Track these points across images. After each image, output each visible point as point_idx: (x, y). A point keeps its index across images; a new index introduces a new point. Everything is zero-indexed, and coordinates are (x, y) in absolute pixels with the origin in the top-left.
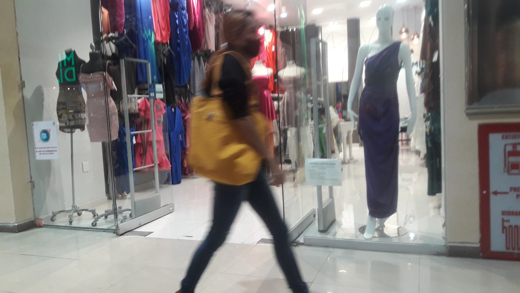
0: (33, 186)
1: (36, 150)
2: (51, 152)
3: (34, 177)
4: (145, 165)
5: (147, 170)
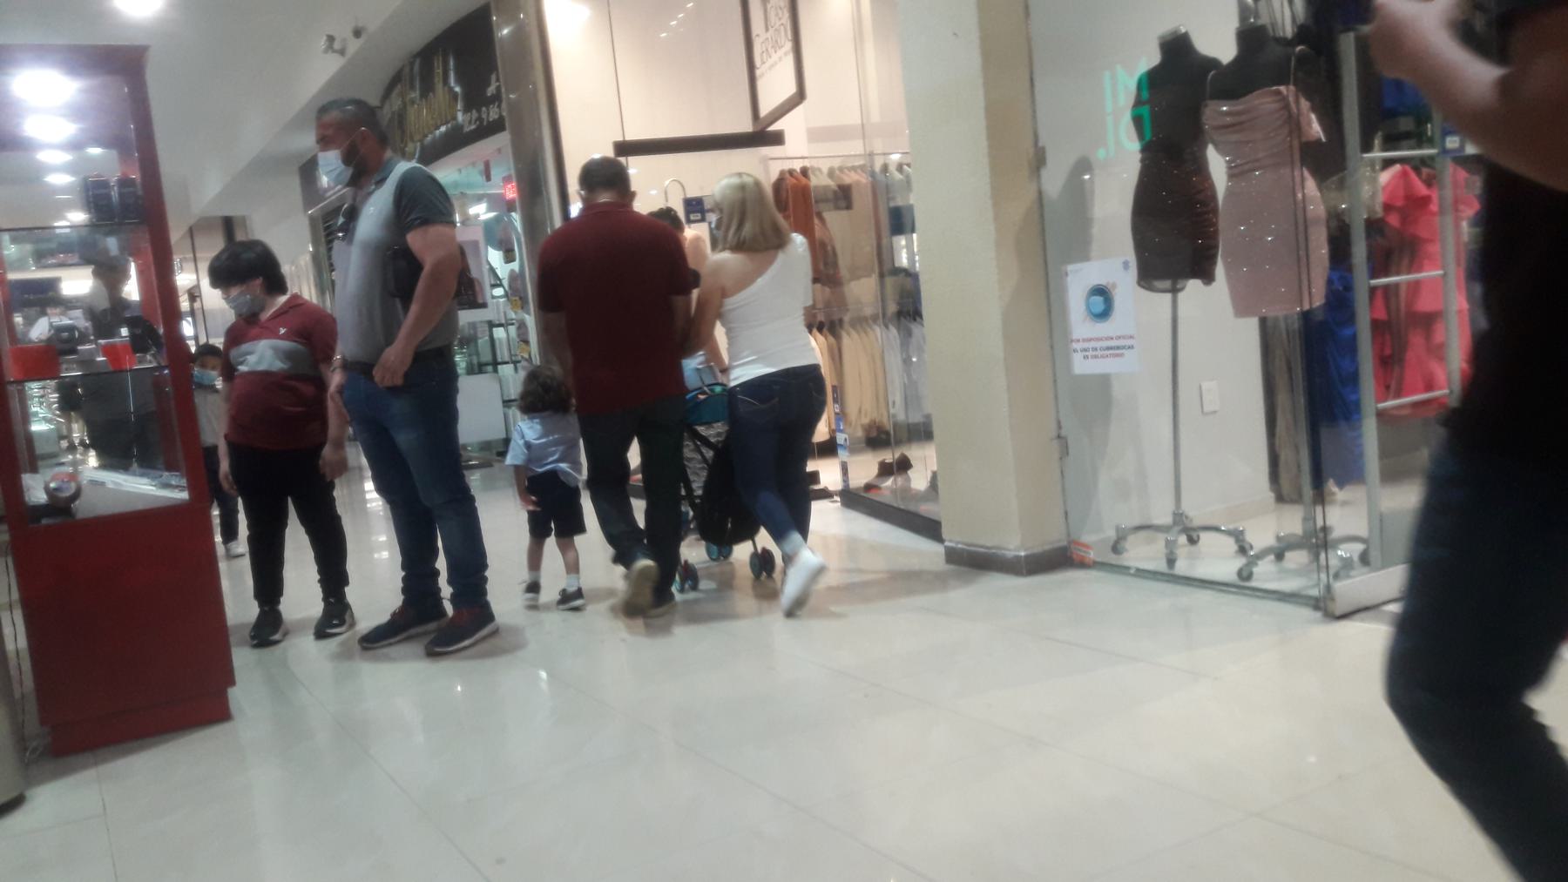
0: (1065, 451)
1: (1075, 345)
2: (1116, 351)
3: (1072, 421)
4: (1398, 395)
5: (1405, 412)
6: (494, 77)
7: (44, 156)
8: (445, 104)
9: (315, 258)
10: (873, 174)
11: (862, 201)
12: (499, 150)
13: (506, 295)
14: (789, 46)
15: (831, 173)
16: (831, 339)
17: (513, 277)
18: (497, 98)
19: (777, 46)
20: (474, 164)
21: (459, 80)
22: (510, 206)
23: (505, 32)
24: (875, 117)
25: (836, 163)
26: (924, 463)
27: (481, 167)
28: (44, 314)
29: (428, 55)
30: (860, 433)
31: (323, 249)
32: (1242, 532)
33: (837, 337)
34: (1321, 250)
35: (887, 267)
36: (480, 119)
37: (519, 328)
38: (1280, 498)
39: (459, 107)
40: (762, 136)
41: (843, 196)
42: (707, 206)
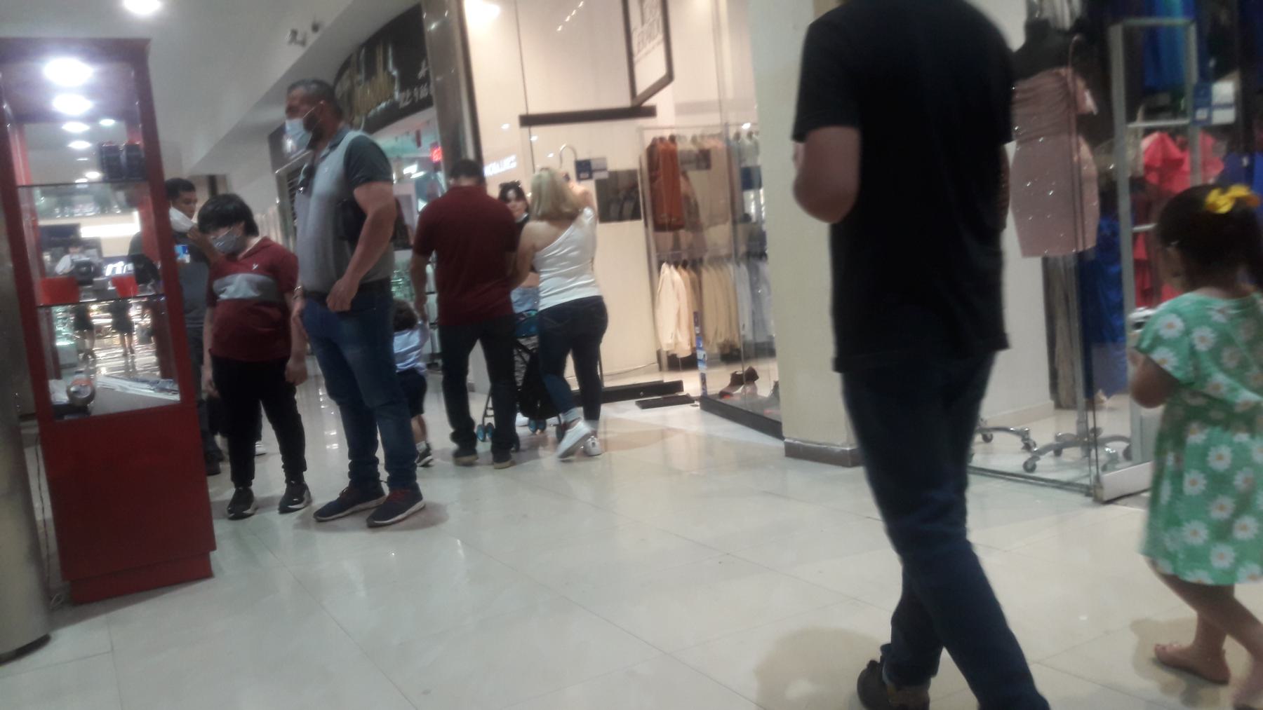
6: (424, 64)
7: (69, 127)
8: (385, 84)
9: (281, 208)
10: (727, 140)
11: (719, 163)
12: (428, 122)
14: (660, 37)
15: (694, 140)
16: (693, 274)
18: (426, 80)
19: (651, 37)
20: (408, 133)
21: (396, 65)
22: (436, 167)
23: (433, 26)
24: (730, 94)
25: (698, 132)
26: (768, 374)
27: (413, 135)
28: (67, 252)
29: (372, 45)
30: (716, 351)
31: (287, 200)
32: (1027, 432)
33: (699, 273)
34: (1093, 203)
35: (738, 216)
36: (412, 96)
38: (1059, 405)
39: (396, 87)
40: (639, 110)
41: (704, 158)
42: (594, 166)
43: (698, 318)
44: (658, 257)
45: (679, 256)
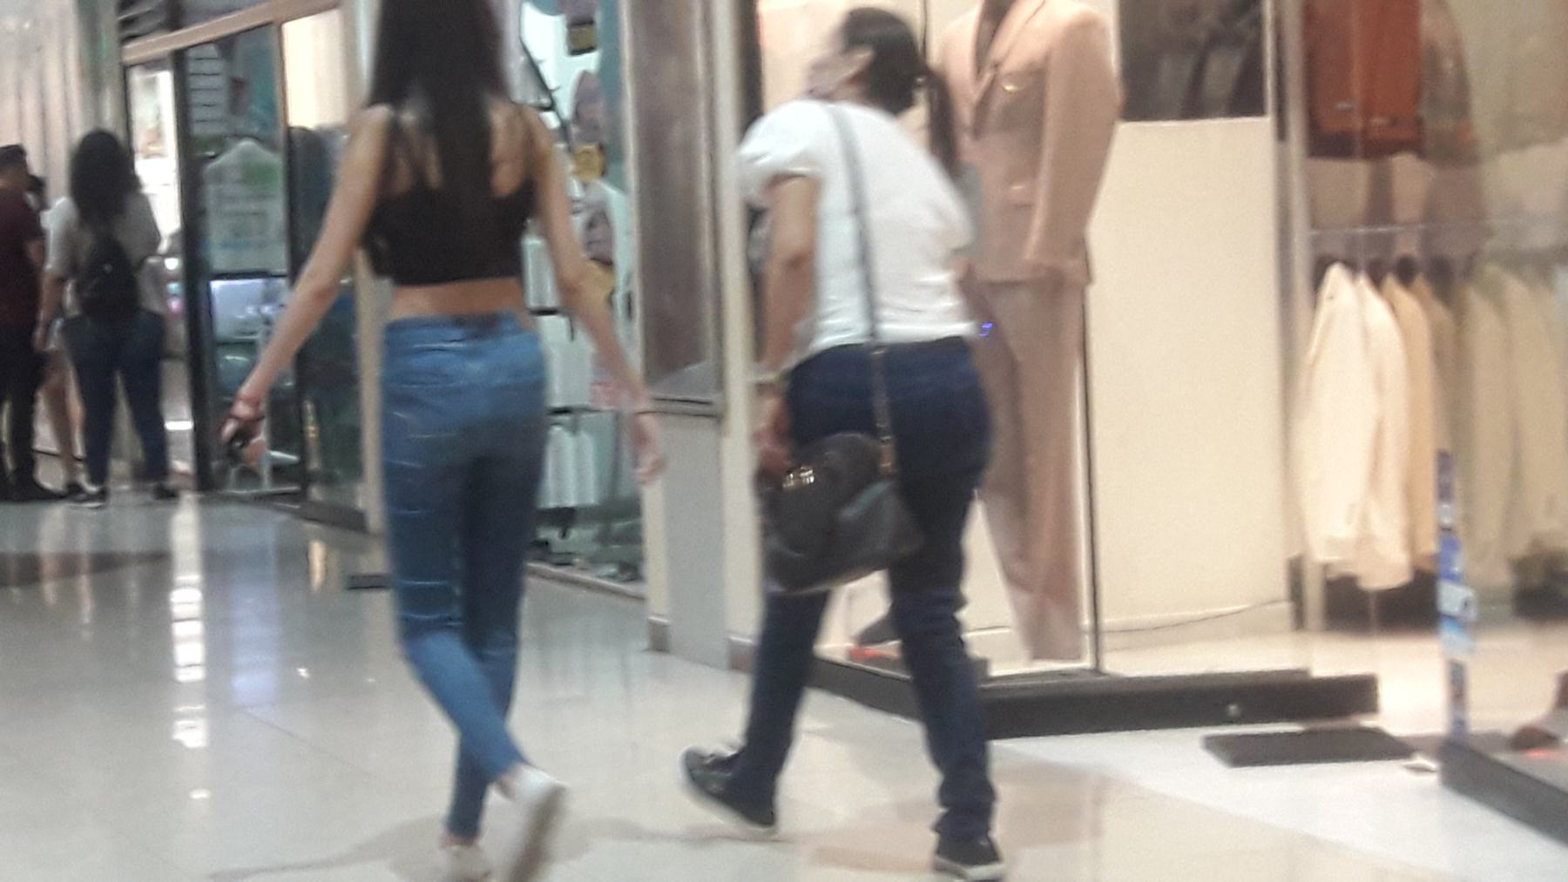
13: (564, 127)
16: (1440, 311)
17: (586, 91)
30: (1503, 578)
37: (591, 225)
43: (1449, 467)
44: (1315, 243)
45: (1388, 240)
